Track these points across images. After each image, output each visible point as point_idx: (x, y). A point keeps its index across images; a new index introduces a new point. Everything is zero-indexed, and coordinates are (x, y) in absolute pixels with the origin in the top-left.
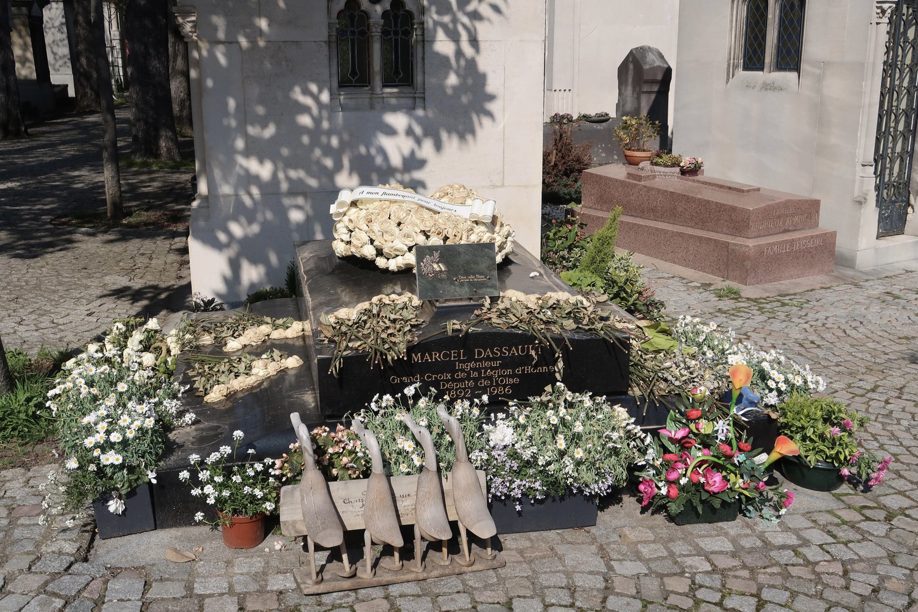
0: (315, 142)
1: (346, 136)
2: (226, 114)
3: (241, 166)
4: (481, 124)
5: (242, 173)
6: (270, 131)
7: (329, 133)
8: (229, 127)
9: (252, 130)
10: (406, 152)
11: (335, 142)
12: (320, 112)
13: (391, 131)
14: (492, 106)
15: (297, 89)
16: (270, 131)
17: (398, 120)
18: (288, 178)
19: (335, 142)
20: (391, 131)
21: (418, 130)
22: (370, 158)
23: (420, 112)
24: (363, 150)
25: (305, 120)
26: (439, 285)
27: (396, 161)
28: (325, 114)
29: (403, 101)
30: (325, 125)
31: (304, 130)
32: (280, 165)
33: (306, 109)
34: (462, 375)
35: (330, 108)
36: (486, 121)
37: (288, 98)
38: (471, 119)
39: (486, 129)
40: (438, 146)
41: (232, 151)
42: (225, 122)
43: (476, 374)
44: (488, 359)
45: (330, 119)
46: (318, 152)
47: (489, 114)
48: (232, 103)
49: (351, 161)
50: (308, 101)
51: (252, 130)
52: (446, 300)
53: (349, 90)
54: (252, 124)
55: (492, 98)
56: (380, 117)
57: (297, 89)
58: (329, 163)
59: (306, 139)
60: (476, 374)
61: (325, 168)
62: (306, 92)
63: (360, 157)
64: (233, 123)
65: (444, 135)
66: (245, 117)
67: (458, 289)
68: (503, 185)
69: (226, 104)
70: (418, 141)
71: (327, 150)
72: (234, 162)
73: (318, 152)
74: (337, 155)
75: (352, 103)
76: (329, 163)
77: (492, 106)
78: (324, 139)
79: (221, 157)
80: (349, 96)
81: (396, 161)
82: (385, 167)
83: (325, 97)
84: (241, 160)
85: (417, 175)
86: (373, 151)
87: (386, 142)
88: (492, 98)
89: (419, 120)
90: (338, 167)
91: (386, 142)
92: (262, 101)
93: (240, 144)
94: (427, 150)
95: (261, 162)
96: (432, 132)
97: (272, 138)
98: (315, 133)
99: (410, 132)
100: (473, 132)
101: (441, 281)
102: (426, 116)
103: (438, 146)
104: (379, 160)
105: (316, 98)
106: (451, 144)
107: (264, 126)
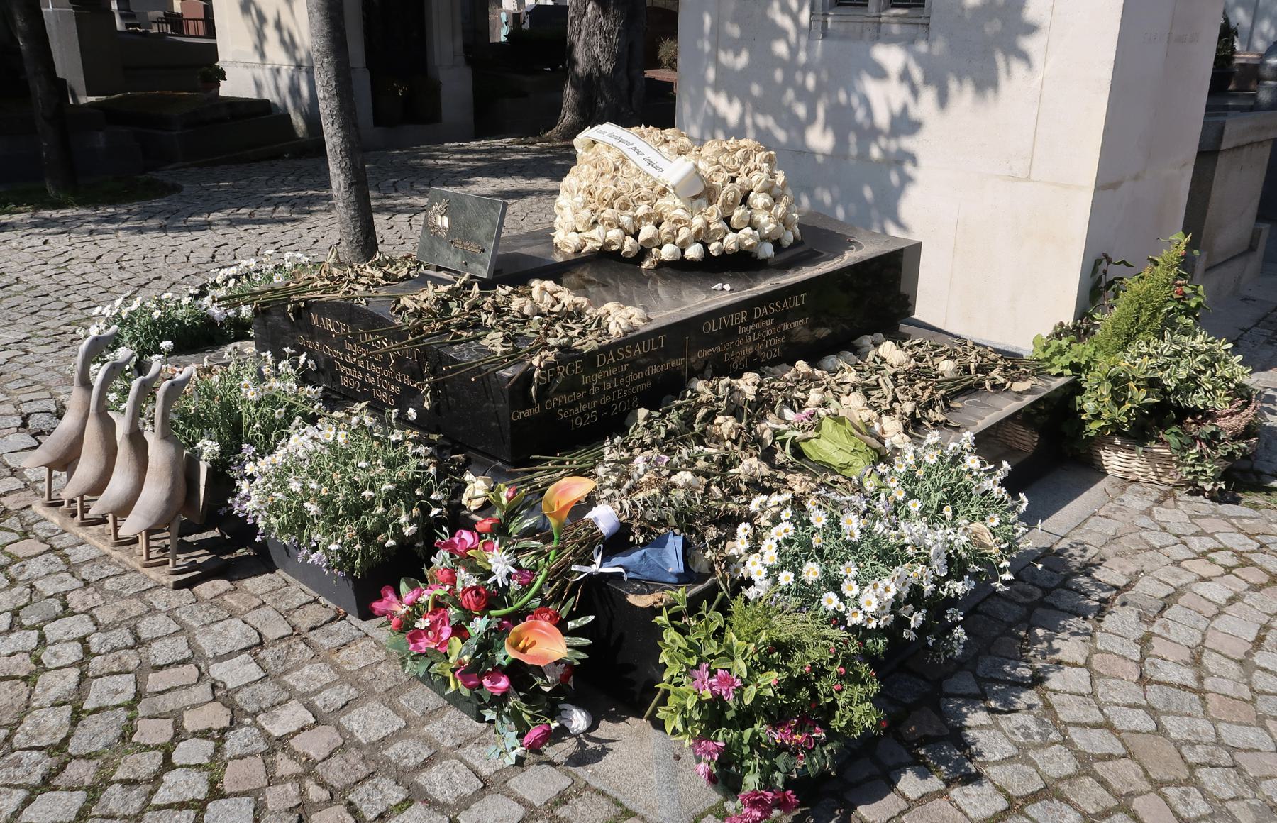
0: (788, 81)
1: (824, 76)
2: (700, 34)
3: (709, 102)
4: (1008, 72)
5: (710, 112)
6: (742, 60)
7: (806, 69)
8: (703, 49)
9: (726, 58)
10: (897, 107)
11: (811, 82)
13: (880, 73)
14: (1030, 44)
16: (742, 60)
17: (891, 57)
18: (755, 126)
19: (811, 82)
20: (880, 73)
21: (917, 74)
22: (849, 109)
24: (842, 97)
25: (781, 48)
26: (437, 245)
28: (803, 41)
30: (802, 57)
31: (779, 61)
32: (749, 106)
33: (782, 34)
35: (809, 33)
36: (1018, 68)
37: (765, 17)
38: (994, 62)
39: (1016, 82)
40: (943, 100)
41: (701, 83)
42: (699, 44)
45: (809, 49)
46: (790, 94)
47: (1024, 57)
48: (707, 20)
49: (827, 112)
50: (785, 22)
51: (726, 58)
52: (439, 269)
53: (842, 10)
54: (725, 50)
55: (1031, 29)
56: (868, 52)
59: (779, 75)
61: (796, 117)
62: (785, 9)
63: (838, 103)
64: (707, 47)
65: (953, 86)
66: (720, 40)
68: (1028, 179)
69: (702, 23)
70: (915, 92)
71: (802, 94)
72: (701, 96)
73: (790, 94)
74: (810, 99)
75: (842, 28)
76: (801, 110)
77: (1030, 44)
78: (799, 77)
79: (693, 90)
80: (838, 18)
82: (867, 125)
83: (805, 17)
84: (710, 94)
85: (908, 143)
86: (855, 101)
87: (872, 88)
88: (1031, 29)
89: (919, 59)
90: (811, 118)
91: (872, 88)
92: (735, 20)
93: (711, 74)
94: (925, 107)
95: (730, 101)
96: (937, 79)
97: (743, 71)
98: (790, 66)
99: (905, 76)
101: (440, 239)
102: (929, 54)
103: (943, 100)
104: (860, 115)
105: (795, 19)
106: (963, 96)
107: (737, 54)
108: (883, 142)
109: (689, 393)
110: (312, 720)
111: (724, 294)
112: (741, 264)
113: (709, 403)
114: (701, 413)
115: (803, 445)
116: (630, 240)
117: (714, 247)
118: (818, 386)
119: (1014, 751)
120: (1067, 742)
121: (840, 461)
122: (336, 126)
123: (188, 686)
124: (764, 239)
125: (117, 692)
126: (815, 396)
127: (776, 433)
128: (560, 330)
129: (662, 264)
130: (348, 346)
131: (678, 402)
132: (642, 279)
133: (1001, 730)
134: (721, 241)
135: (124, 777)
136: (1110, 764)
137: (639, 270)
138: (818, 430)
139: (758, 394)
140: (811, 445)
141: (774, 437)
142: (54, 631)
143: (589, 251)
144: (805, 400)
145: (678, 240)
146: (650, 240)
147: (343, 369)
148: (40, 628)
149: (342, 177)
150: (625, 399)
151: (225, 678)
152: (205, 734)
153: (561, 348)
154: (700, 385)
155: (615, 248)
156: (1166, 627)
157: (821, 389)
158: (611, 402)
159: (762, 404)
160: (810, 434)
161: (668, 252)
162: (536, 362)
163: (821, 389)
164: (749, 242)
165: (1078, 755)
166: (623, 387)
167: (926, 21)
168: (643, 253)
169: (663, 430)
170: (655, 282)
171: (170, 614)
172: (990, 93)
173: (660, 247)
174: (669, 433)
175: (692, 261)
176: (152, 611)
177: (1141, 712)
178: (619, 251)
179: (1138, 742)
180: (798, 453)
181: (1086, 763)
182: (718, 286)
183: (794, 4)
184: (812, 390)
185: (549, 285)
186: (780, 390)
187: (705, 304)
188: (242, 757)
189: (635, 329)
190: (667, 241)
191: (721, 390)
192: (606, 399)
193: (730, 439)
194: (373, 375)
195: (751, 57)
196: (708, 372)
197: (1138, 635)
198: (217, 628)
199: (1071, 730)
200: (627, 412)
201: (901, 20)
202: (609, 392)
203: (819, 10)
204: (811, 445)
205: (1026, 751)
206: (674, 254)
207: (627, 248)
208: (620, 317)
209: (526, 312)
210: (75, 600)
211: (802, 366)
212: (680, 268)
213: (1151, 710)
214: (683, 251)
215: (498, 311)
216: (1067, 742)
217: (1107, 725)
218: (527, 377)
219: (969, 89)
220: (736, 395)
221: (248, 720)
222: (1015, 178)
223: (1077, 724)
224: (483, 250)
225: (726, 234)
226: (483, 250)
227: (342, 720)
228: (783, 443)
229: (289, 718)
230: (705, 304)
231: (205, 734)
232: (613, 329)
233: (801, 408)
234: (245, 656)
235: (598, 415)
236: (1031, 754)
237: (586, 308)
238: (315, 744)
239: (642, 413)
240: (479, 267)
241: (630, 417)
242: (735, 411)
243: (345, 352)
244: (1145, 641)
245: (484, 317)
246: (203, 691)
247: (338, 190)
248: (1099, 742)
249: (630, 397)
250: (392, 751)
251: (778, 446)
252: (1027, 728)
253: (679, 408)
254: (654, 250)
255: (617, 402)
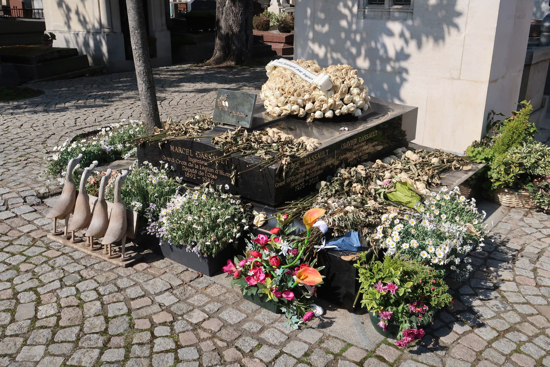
0: (348, 37)
1: (364, 35)
2: (306, 17)
3: (310, 48)
4: (449, 33)
5: (310, 52)
6: (326, 29)
7: (356, 32)
8: (307, 24)
9: (318, 28)
10: (398, 48)
11: (358, 38)
12: (352, 19)
13: (390, 34)
14: (458, 21)
15: (341, 4)
16: (326, 29)
17: (396, 27)
18: (332, 58)
19: (358, 38)
20: (390, 34)
21: (407, 34)
22: (376, 49)
23: (410, 22)
24: (373, 44)
25: (344, 23)
26: (223, 114)
27: (392, 53)
28: (354, 20)
29: (403, 14)
30: (354, 27)
31: (343, 29)
32: (329, 49)
33: (344, 17)
34: (192, 165)
35: (357, 16)
36: (453, 31)
37: (336, 9)
38: (443, 29)
39: (453, 37)
40: (419, 45)
41: (307, 39)
42: (305, 22)
43: (197, 167)
44: (202, 159)
45: (357, 23)
46: (348, 43)
47: (456, 26)
48: (309, 11)
49: (366, 51)
50: (346, 11)
51: (318, 28)
52: (224, 124)
54: (318, 24)
55: (459, 14)
56: (385, 25)
57: (341, 4)
58: (354, 51)
59: (343, 35)
60: (197, 167)
62: (346, 6)
63: (371, 47)
64: (309, 23)
65: (424, 39)
66: (315, 20)
67: (231, 119)
68: (459, 79)
69: (306, 12)
70: (407, 42)
71: (354, 43)
72: (306, 45)
73: (348, 43)
74: (358, 46)
76: (354, 51)
77: (458, 21)
78: (352, 36)
80: (370, 10)
81: (392, 53)
82: (384, 57)
83: (355, 9)
84: (310, 44)
85: (404, 64)
86: (379, 46)
87: (387, 41)
88: (459, 14)
89: (408, 27)
90: (359, 54)
91: (387, 41)
92: (322, 11)
93: (311, 35)
95: (320, 46)
97: (327, 33)
98: (348, 31)
99: (402, 35)
100: (443, 38)
101: (224, 112)
102: (413, 25)
103: (419, 45)
104: (382, 52)
105: (350, 10)
106: (429, 44)
107: (323, 26)
108: (392, 64)
109: (339, 174)
110: (208, 316)
111: (345, 132)
112: (348, 119)
113: (348, 178)
114: (347, 182)
115: (388, 195)
116: (302, 110)
117: (337, 112)
118: (387, 170)
119: (495, 314)
120: (515, 310)
121: (406, 201)
122: (141, 62)
123: (149, 306)
124: (357, 108)
125: (120, 310)
126: (387, 174)
127: (376, 190)
128: (288, 149)
129: (315, 120)
130: (190, 159)
131: (336, 178)
132: (306, 126)
133: (487, 307)
134: (341, 109)
135: (138, 342)
136: (533, 317)
137: (306, 123)
138: (395, 188)
139: (367, 174)
140: (393, 195)
141: (375, 191)
142: (82, 286)
143: (284, 115)
144: (384, 176)
145: (323, 109)
146: (310, 110)
147: (186, 169)
148: (75, 286)
149: (144, 85)
150: (314, 178)
151: (163, 302)
152: (164, 324)
153: (291, 156)
154: (343, 171)
155: (295, 113)
156: (541, 265)
157: (389, 171)
158: (309, 179)
159: (368, 179)
160: (392, 189)
161: (318, 114)
162: (284, 162)
163: (389, 171)
164: (352, 109)
165: (520, 314)
166: (313, 172)
167: (411, 11)
168: (307, 115)
169: (334, 190)
170: (312, 128)
171: (128, 277)
172: (441, 42)
173: (314, 112)
174: (336, 191)
175: (328, 118)
176: (119, 277)
177: (540, 297)
178: (297, 115)
179: (542, 309)
180: (386, 197)
181: (524, 317)
182: (342, 128)
183: (350, 4)
184: (386, 172)
185: (275, 130)
186: (374, 172)
187: (340, 136)
188: (184, 332)
189: (317, 148)
190: (318, 110)
191: (352, 173)
192: (307, 178)
193: (360, 193)
194: (203, 171)
195: (330, 27)
196: (343, 165)
197: (531, 268)
198: (151, 282)
199: (515, 305)
200: (317, 182)
201: (399, 11)
202: (308, 175)
203: (362, 6)
204: (393, 195)
205: (499, 314)
206: (321, 115)
207: (301, 113)
208: (311, 142)
209: (269, 141)
210: (84, 273)
211: (379, 162)
212: (323, 121)
213: (543, 296)
214: (324, 114)
215: (256, 141)
216: (515, 310)
217: (528, 303)
218: (281, 169)
219: (431, 41)
220: (358, 175)
221: (180, 318)
222: (453, 79)
223: (516, 303)
224: (247, 116)
225: (343, 106)
226: (247, 116)
227: (220, 315)
228: (379, 194)
229: (197, 317)
230: (340, 136)
231: (164, 324)
232: (308, 148)
233: (383, 180)
234: (167, 293)
235: (305, 184)
236: (502, 315)
237: (294, 139)
238: (213, 325)
239: (323, 183)
240: (245, 123)
241: (317, 185)
242: (359, 181)
243: (188, 162)
244: (535, 270)
245: (253, 144)
246: (156, 308)
247: (142, 91)
248: (526, 309)
249: (316, 177)
250: (246, 326)
251: (378, 196)
252: (497, 305)
253: (337, 181)
254: (312, 114)
255: (311, 179)
